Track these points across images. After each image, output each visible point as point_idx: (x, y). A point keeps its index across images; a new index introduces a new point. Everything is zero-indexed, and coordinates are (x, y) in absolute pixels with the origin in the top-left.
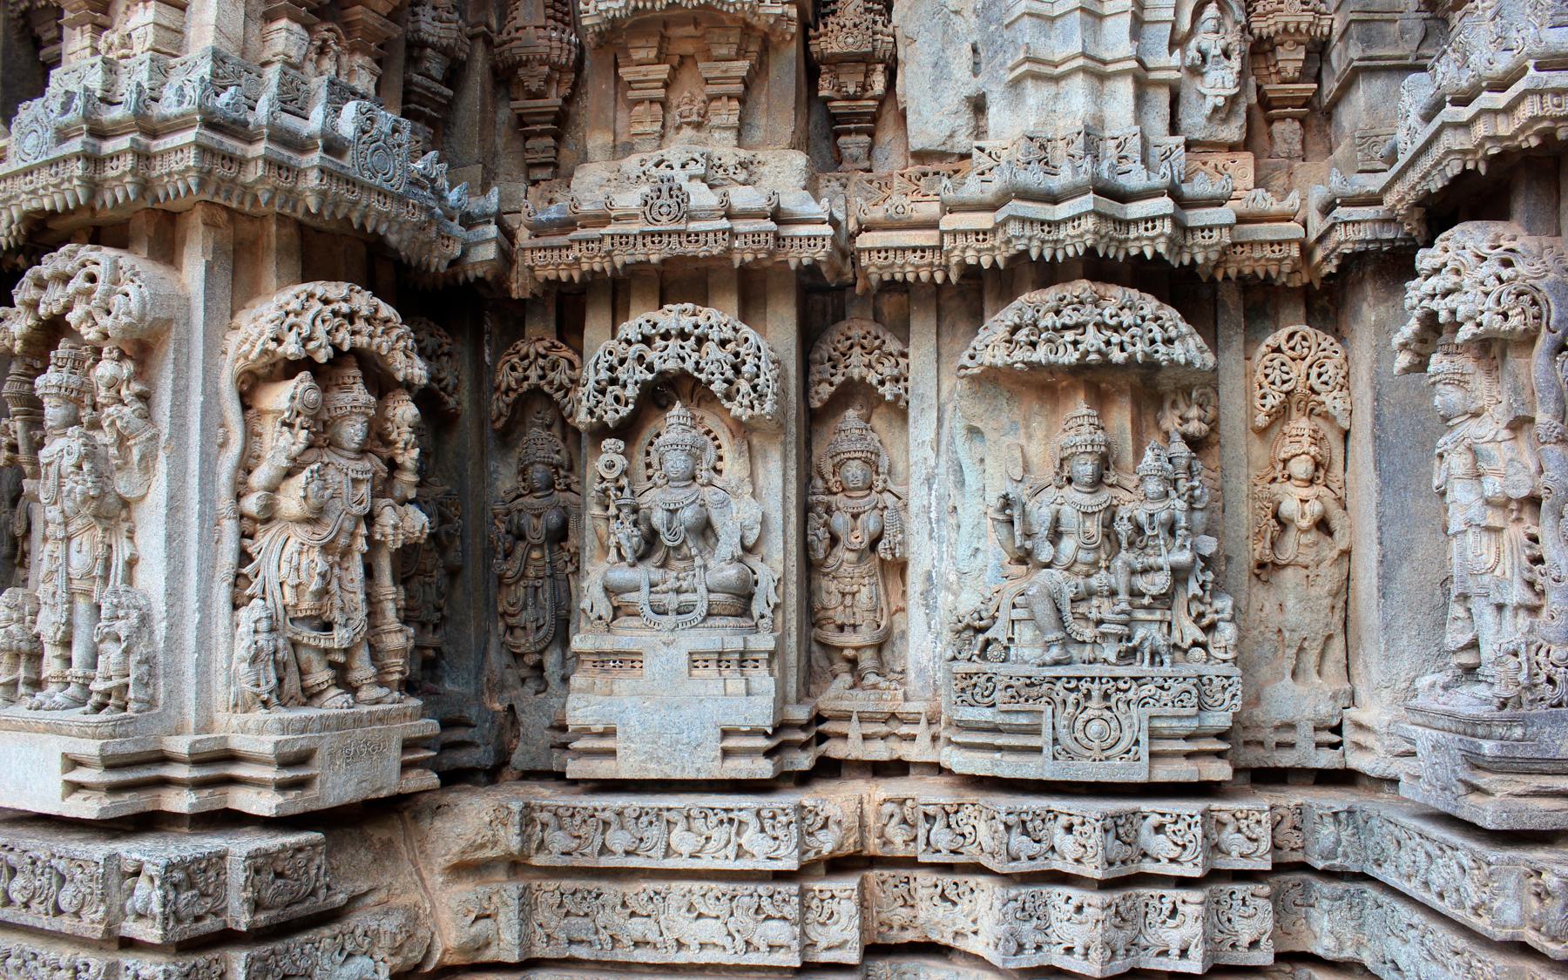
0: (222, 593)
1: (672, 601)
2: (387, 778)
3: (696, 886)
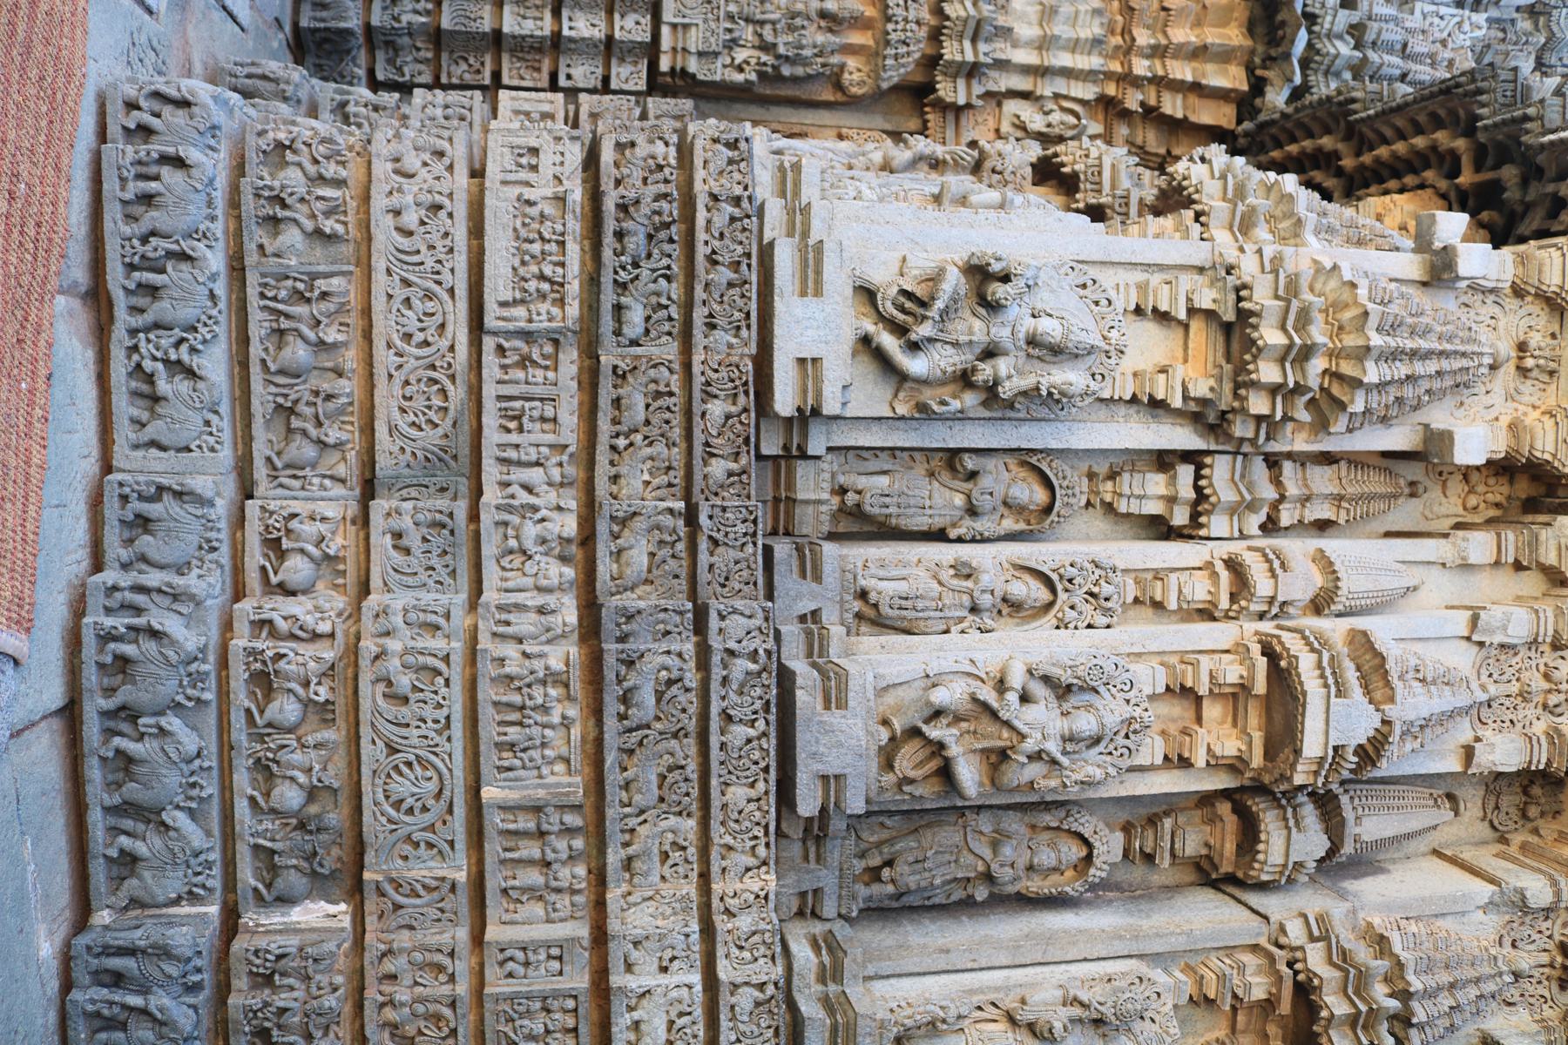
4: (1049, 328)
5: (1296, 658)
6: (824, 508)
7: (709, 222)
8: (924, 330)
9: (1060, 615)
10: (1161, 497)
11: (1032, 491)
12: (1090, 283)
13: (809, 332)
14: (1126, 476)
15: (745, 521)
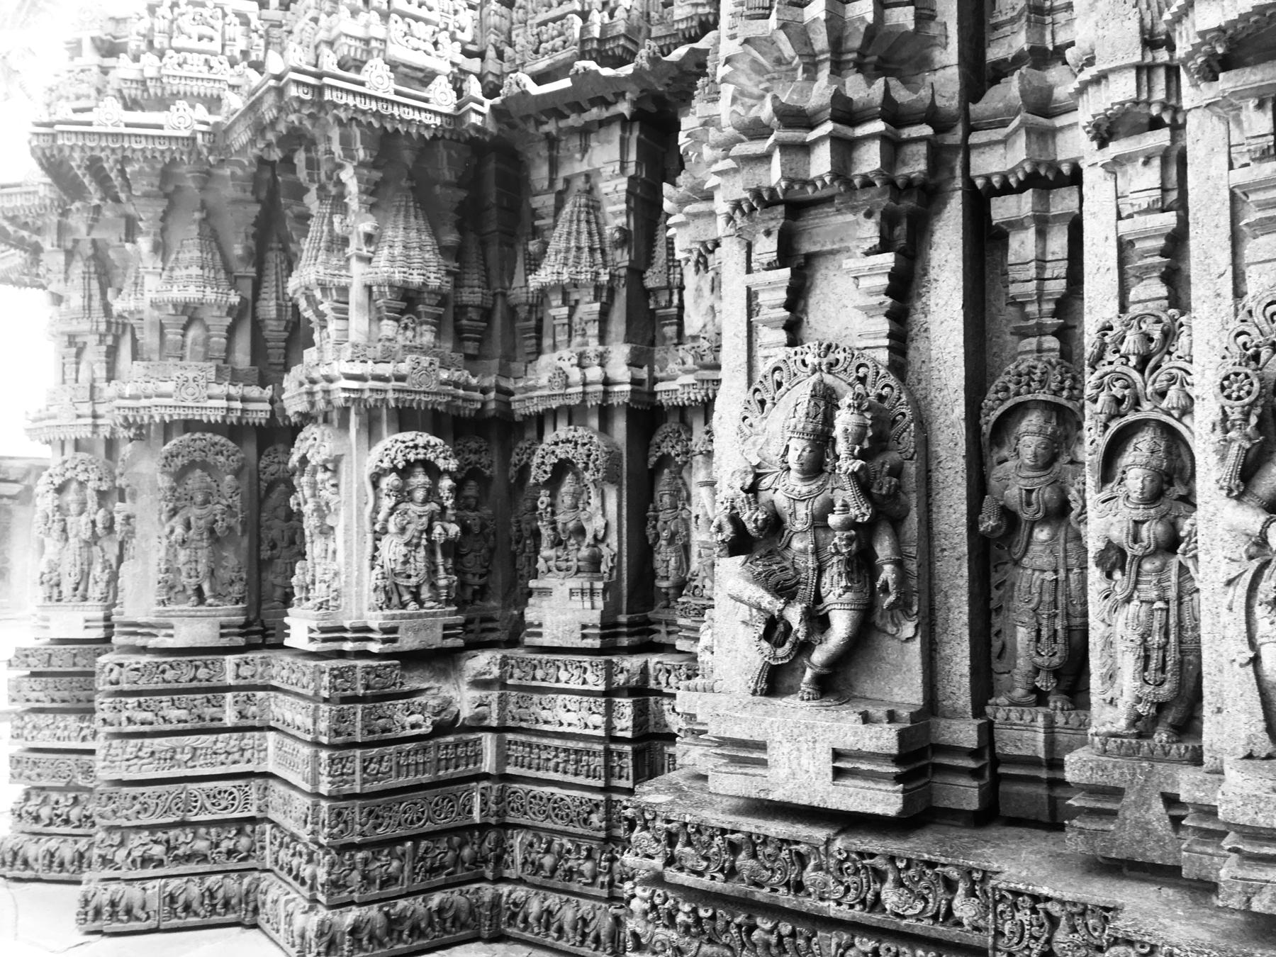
0: (367, 563)
1: (563, 565)
2: (435, 638)
3: (568, 697)
4: (799, 449)
5: (1202, 34)
6: (1060, 719)
7: (694, 872)
8: (794, 615)
9: (1176, 413)
10: (1042, 234)
11: (1027, 433)
12: (758, 396)
13: (804, 761)
14: (1014, 289)
15: (1015, 906)
